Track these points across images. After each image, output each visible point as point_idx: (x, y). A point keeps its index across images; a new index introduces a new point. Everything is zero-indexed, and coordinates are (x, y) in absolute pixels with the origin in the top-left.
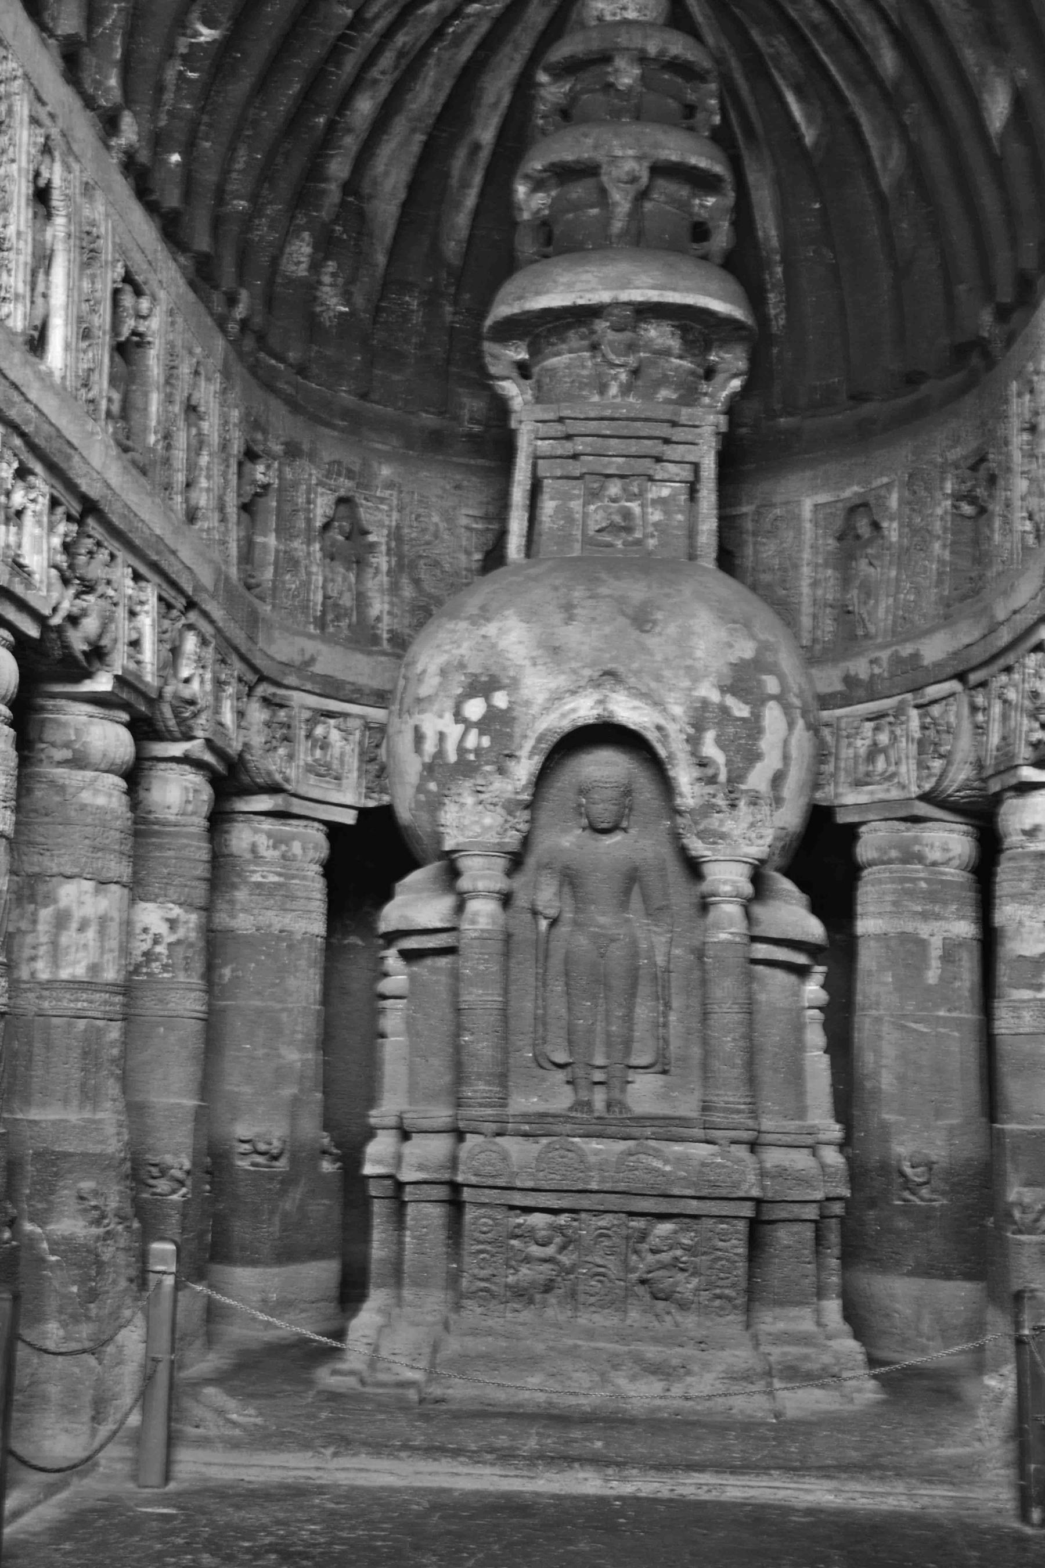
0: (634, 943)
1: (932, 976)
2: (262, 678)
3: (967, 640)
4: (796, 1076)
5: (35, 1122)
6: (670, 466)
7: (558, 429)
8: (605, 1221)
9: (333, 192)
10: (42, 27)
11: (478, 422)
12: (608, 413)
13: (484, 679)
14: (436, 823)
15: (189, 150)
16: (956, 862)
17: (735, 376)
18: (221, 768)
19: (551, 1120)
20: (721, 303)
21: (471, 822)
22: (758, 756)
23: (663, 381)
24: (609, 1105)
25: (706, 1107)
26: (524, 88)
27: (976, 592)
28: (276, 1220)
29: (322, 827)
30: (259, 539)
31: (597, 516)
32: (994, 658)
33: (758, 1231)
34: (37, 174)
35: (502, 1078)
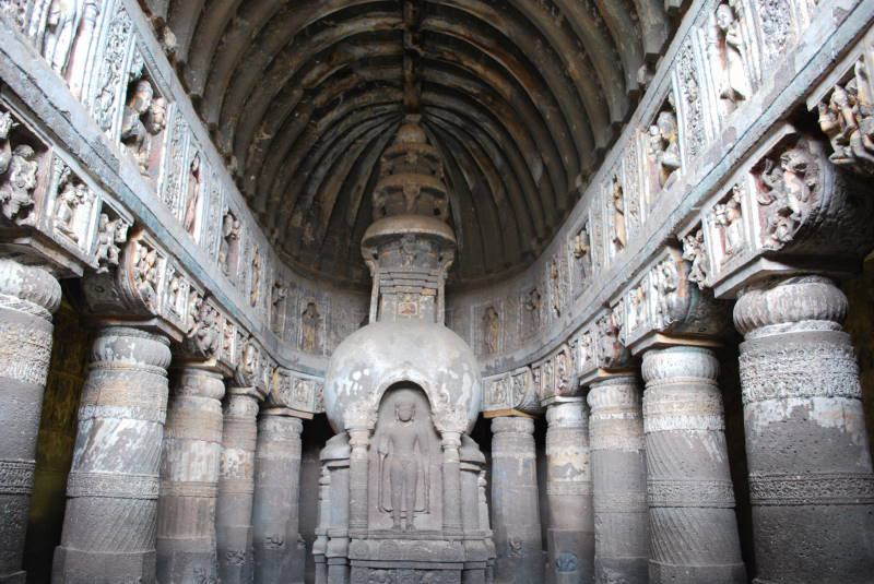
0: (416, 463)
2: (279, 366)
3: (531, 352)
4: (476, 513)
5: (177, 540)
7: (388, 276)
8: (406, 572)
9: (310, 200)
10: (202, 119)
14: (342, 418)
15: (259, 175)
18: (262, 398)
20: (445, 234)
21: (355, 418)
22: (462, 393)
23: (426, 260)
24: (408, 527)
25: (444, 527)
26: (377, 165)
27: (534, 335)
30: (280, 316)
31: (402, 306)
32: (543, 358)
33: (464, 574)
34: (192, 165)
35: (367, 517)
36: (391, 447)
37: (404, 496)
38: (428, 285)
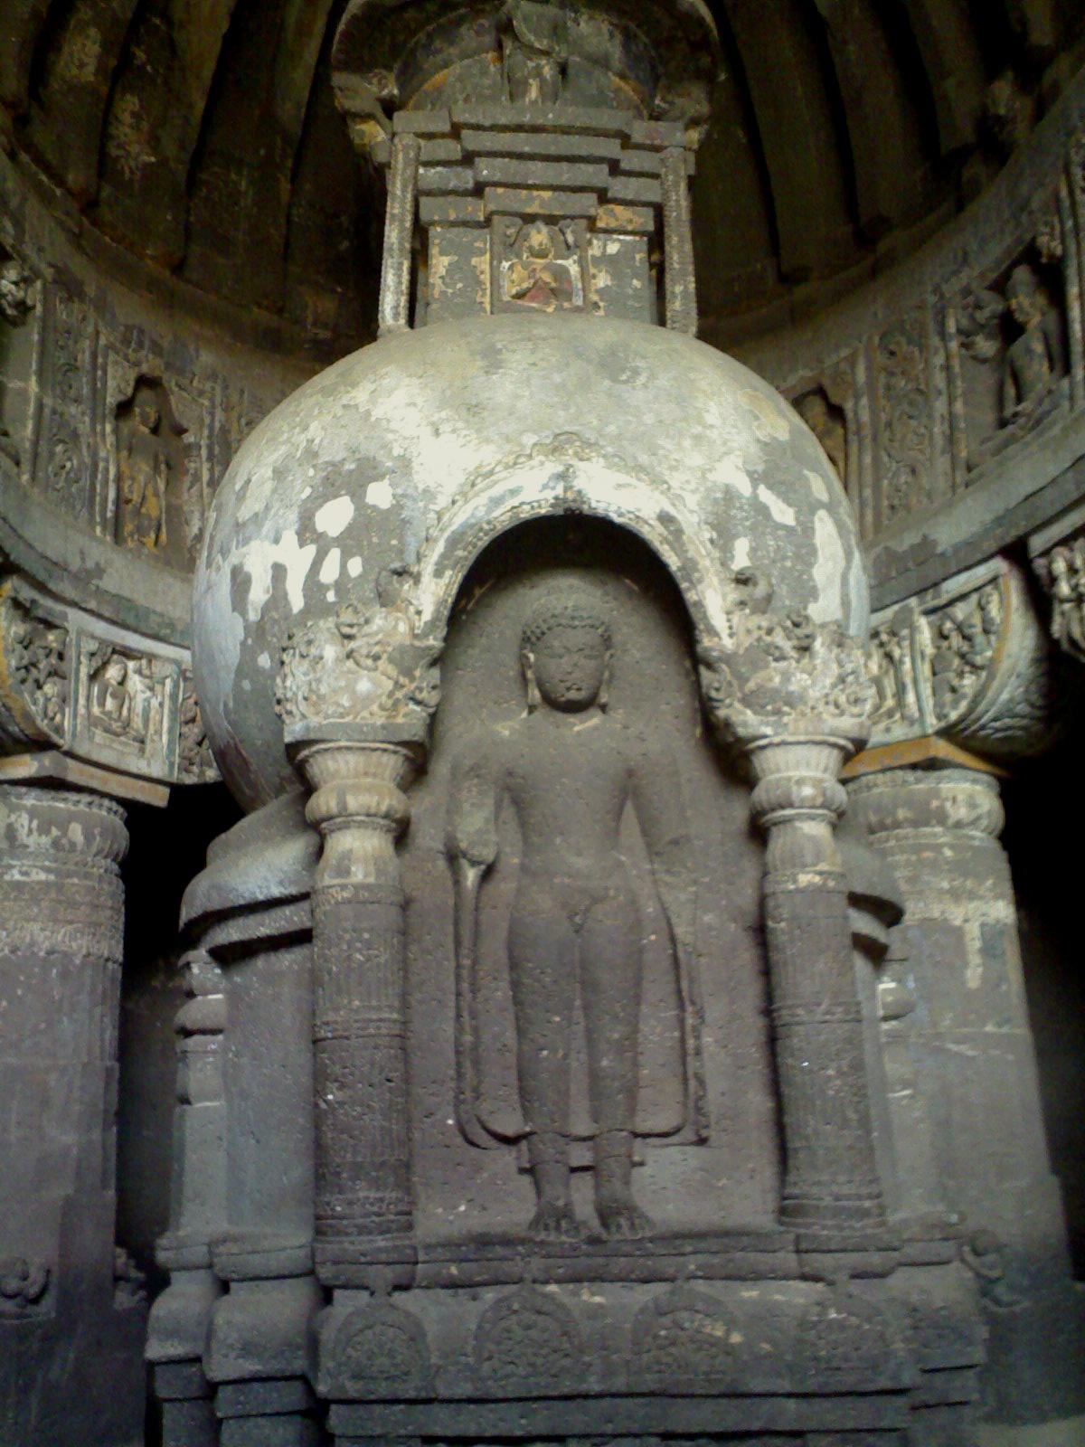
0: (633, 902)
1: (973, 975)
3: (1030, 489)
6: (619, 209)
7: (452, 149)
11: (325, 326)
12: (527, 119)
13: (350, 466)
16: (984, 822)
17: (694, 122)
19: (499, 1250)
22: (813, 594)
23: (600, 101)
24: (607, 1213)
28: (34, 1402)
29: (114, 806)
30: (14, 385)
31: (514, 277)
36: (512, 827)
37: (578, 1063)
38: (618, 187)
